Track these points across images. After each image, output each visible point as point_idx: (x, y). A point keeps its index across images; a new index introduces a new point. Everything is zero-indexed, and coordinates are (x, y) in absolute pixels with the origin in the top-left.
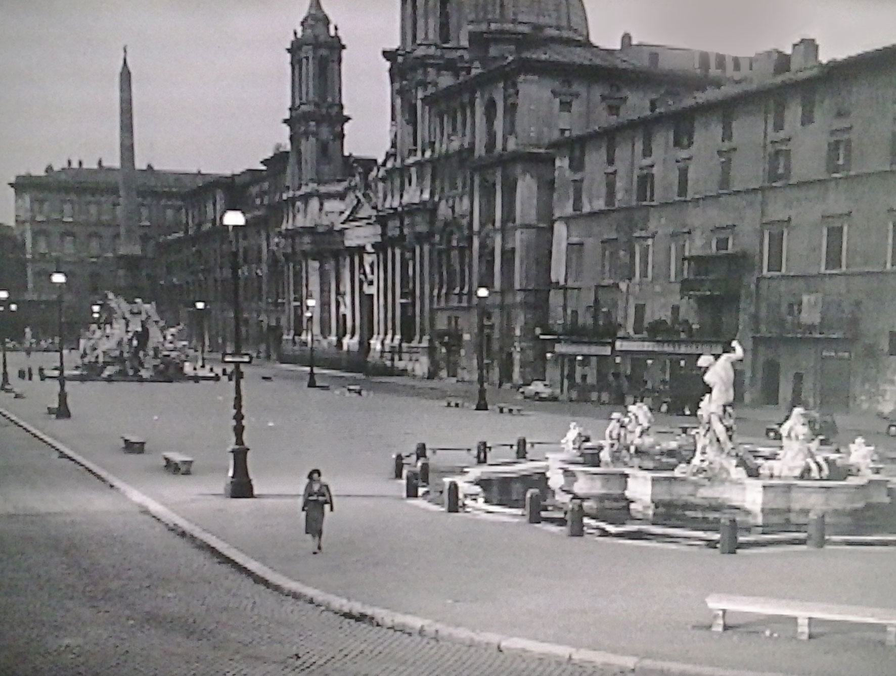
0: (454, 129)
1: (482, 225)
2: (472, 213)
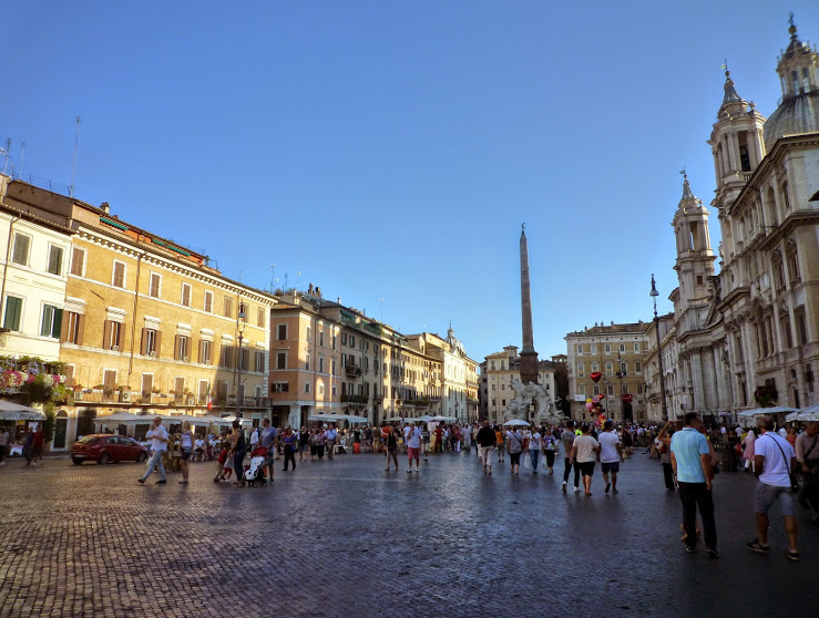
1: (779, 292)
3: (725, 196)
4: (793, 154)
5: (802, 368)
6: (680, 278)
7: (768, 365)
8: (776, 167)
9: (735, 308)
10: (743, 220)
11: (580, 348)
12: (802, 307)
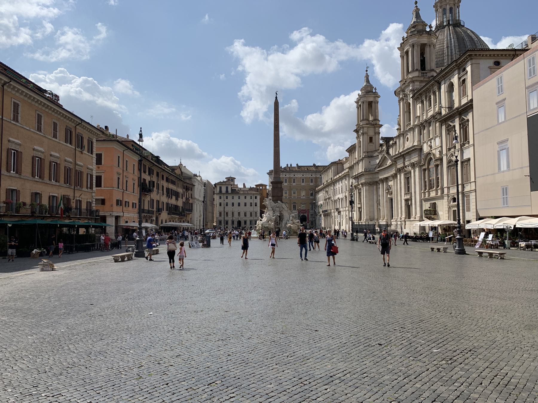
0: (430, 105)
2: (441, 147)
6: (358, 137)
7: (433, 194)
8: (459, 69)
10: (422, 102)
12: (469, 160)
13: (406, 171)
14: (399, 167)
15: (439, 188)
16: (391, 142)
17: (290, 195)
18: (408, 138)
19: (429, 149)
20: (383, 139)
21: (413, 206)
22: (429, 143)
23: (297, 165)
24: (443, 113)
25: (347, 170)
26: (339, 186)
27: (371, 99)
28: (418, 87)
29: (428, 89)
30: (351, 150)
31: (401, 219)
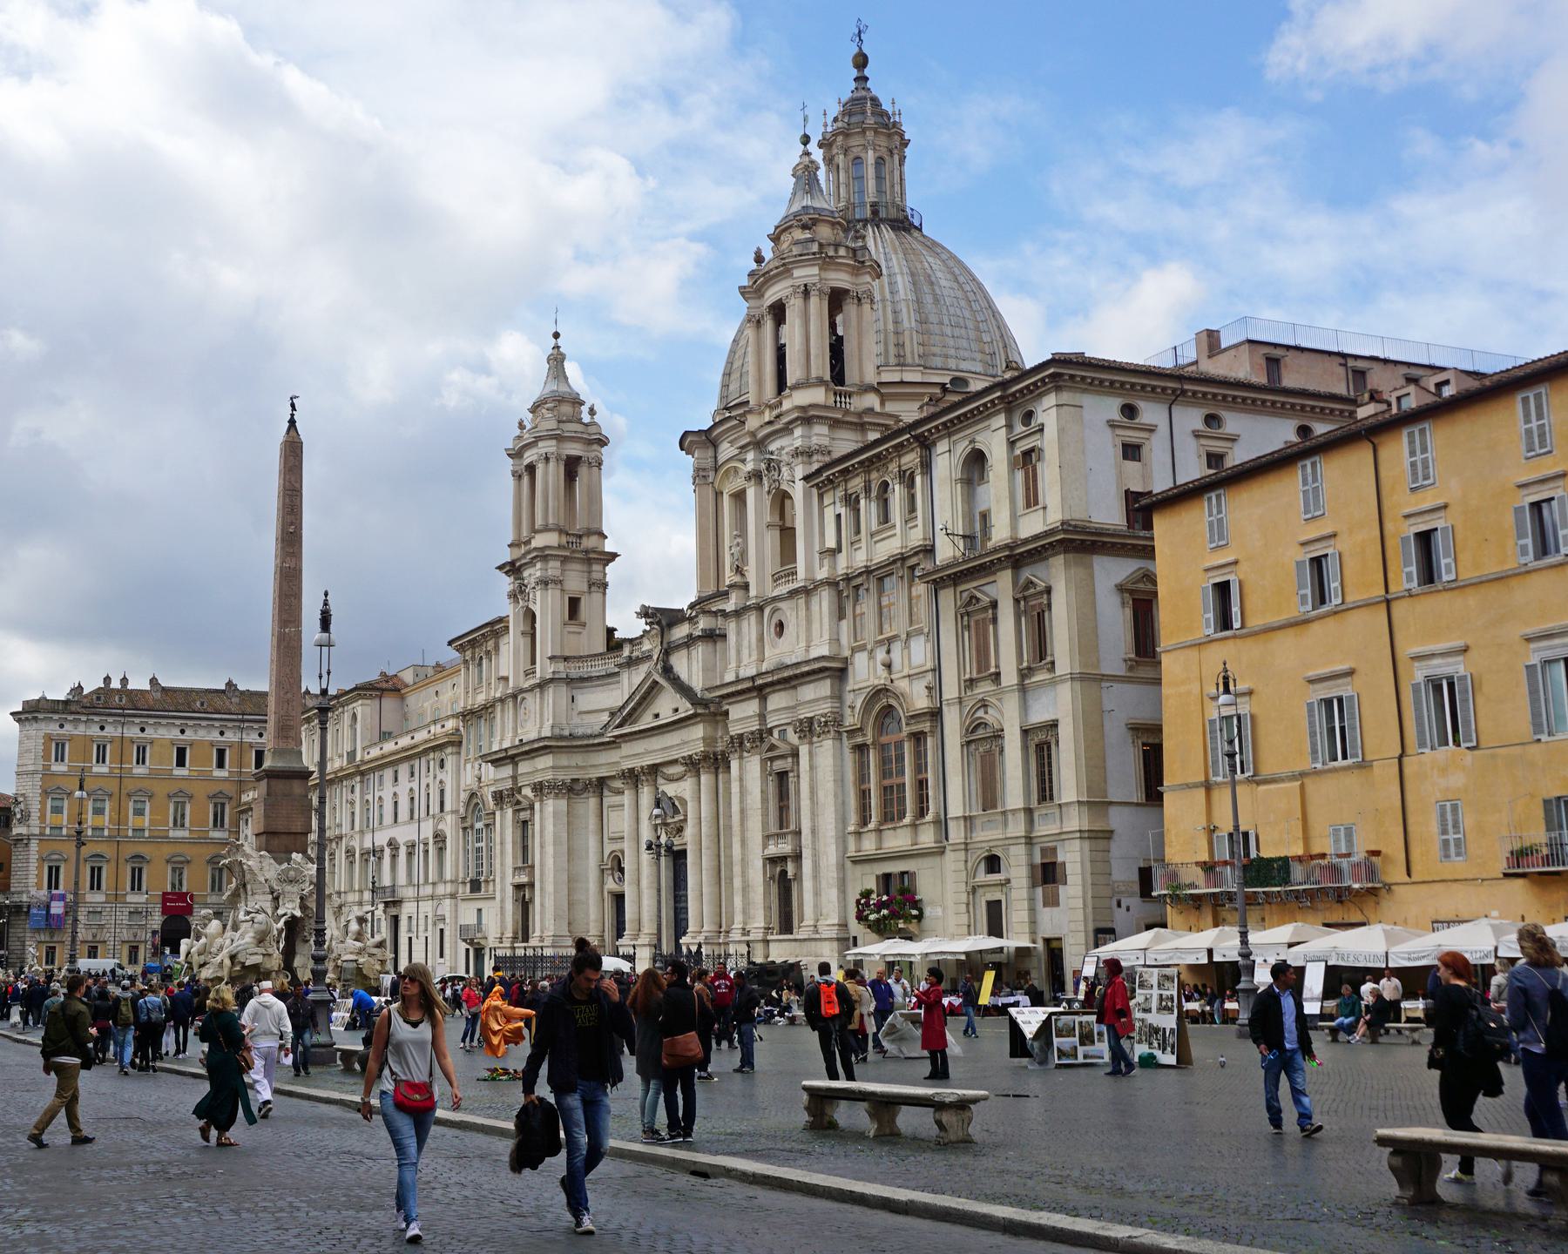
0: (885, 518)
2: (937, 670)
3: (787, 430)
4: (1066, 397)
5: (1030, 855)
6: (517, 594)
7: (898, 840)
8: (1009, 411)
9: (777, 701)
10: (852, 502)
11: (60, 746)
12: (1054, 725)
13: (772, 747)
14: (735, 730)
15: (929, 817)
16: (680, 632)
17: (120, 820)
18: (781, 625)
19: (882, 672)
20: (646, 613)
21: (807, 884)
22: (881, 655)
23: (153, 681)
24: (946, 551)
25: (450, 724)
26: (391, 789)
27: (574, 449)
28: (825, 441)
29: (878, 456)
30: (478, 642)
31: (745, 932)
